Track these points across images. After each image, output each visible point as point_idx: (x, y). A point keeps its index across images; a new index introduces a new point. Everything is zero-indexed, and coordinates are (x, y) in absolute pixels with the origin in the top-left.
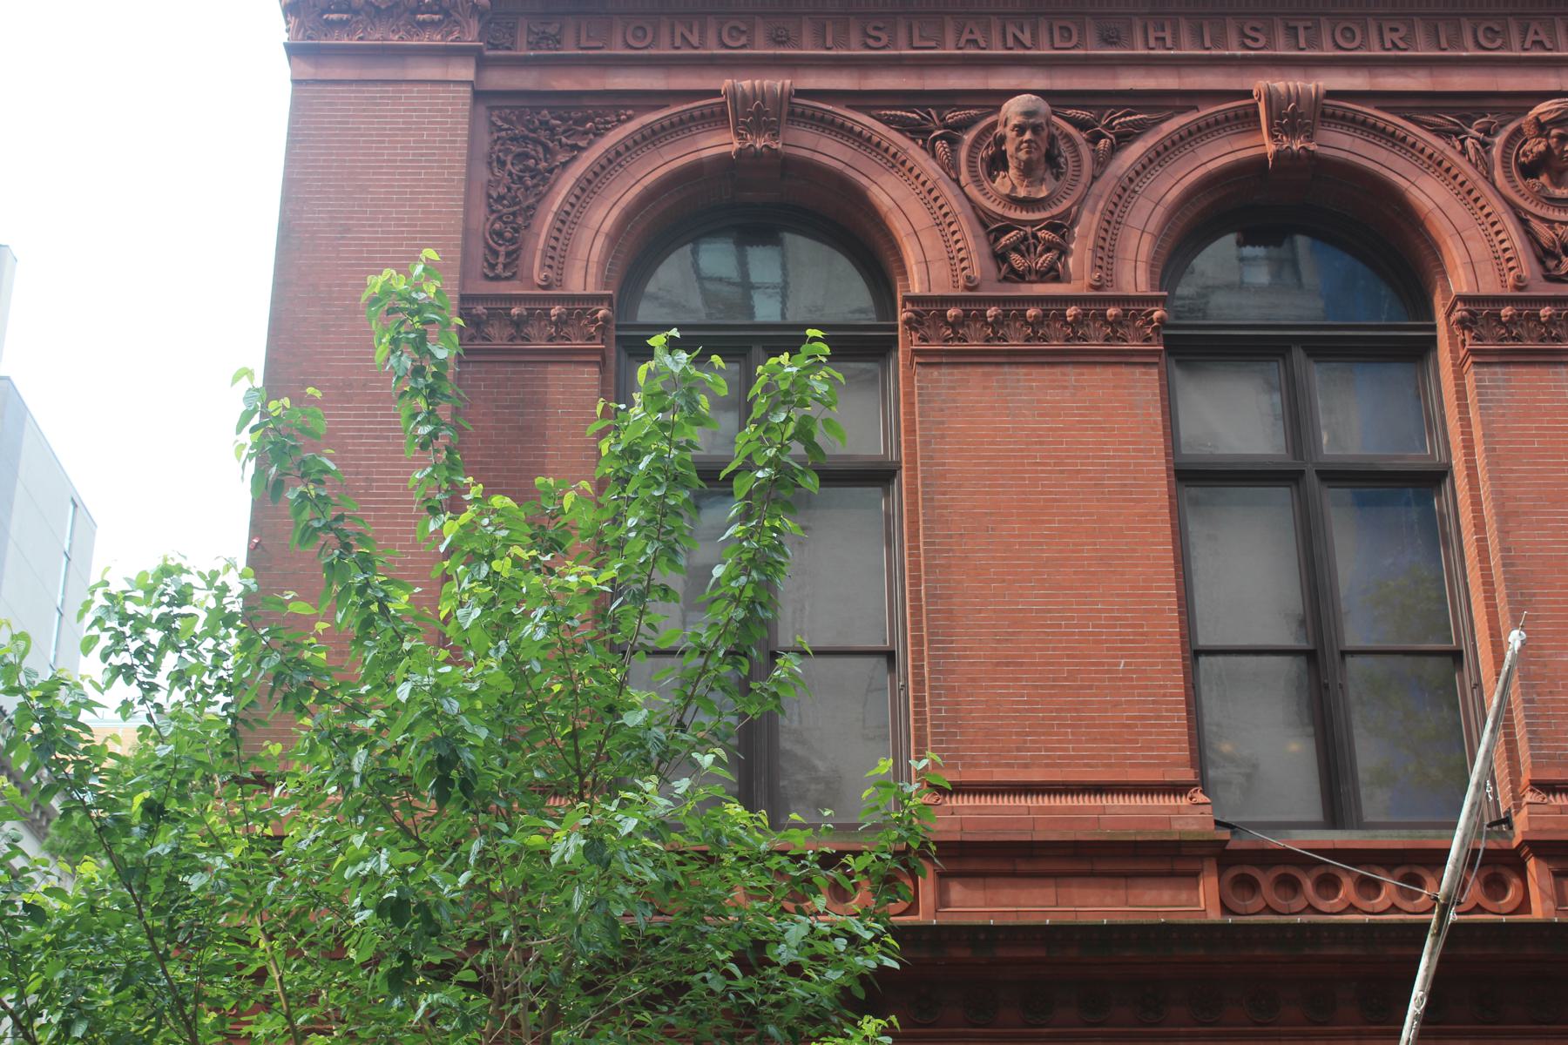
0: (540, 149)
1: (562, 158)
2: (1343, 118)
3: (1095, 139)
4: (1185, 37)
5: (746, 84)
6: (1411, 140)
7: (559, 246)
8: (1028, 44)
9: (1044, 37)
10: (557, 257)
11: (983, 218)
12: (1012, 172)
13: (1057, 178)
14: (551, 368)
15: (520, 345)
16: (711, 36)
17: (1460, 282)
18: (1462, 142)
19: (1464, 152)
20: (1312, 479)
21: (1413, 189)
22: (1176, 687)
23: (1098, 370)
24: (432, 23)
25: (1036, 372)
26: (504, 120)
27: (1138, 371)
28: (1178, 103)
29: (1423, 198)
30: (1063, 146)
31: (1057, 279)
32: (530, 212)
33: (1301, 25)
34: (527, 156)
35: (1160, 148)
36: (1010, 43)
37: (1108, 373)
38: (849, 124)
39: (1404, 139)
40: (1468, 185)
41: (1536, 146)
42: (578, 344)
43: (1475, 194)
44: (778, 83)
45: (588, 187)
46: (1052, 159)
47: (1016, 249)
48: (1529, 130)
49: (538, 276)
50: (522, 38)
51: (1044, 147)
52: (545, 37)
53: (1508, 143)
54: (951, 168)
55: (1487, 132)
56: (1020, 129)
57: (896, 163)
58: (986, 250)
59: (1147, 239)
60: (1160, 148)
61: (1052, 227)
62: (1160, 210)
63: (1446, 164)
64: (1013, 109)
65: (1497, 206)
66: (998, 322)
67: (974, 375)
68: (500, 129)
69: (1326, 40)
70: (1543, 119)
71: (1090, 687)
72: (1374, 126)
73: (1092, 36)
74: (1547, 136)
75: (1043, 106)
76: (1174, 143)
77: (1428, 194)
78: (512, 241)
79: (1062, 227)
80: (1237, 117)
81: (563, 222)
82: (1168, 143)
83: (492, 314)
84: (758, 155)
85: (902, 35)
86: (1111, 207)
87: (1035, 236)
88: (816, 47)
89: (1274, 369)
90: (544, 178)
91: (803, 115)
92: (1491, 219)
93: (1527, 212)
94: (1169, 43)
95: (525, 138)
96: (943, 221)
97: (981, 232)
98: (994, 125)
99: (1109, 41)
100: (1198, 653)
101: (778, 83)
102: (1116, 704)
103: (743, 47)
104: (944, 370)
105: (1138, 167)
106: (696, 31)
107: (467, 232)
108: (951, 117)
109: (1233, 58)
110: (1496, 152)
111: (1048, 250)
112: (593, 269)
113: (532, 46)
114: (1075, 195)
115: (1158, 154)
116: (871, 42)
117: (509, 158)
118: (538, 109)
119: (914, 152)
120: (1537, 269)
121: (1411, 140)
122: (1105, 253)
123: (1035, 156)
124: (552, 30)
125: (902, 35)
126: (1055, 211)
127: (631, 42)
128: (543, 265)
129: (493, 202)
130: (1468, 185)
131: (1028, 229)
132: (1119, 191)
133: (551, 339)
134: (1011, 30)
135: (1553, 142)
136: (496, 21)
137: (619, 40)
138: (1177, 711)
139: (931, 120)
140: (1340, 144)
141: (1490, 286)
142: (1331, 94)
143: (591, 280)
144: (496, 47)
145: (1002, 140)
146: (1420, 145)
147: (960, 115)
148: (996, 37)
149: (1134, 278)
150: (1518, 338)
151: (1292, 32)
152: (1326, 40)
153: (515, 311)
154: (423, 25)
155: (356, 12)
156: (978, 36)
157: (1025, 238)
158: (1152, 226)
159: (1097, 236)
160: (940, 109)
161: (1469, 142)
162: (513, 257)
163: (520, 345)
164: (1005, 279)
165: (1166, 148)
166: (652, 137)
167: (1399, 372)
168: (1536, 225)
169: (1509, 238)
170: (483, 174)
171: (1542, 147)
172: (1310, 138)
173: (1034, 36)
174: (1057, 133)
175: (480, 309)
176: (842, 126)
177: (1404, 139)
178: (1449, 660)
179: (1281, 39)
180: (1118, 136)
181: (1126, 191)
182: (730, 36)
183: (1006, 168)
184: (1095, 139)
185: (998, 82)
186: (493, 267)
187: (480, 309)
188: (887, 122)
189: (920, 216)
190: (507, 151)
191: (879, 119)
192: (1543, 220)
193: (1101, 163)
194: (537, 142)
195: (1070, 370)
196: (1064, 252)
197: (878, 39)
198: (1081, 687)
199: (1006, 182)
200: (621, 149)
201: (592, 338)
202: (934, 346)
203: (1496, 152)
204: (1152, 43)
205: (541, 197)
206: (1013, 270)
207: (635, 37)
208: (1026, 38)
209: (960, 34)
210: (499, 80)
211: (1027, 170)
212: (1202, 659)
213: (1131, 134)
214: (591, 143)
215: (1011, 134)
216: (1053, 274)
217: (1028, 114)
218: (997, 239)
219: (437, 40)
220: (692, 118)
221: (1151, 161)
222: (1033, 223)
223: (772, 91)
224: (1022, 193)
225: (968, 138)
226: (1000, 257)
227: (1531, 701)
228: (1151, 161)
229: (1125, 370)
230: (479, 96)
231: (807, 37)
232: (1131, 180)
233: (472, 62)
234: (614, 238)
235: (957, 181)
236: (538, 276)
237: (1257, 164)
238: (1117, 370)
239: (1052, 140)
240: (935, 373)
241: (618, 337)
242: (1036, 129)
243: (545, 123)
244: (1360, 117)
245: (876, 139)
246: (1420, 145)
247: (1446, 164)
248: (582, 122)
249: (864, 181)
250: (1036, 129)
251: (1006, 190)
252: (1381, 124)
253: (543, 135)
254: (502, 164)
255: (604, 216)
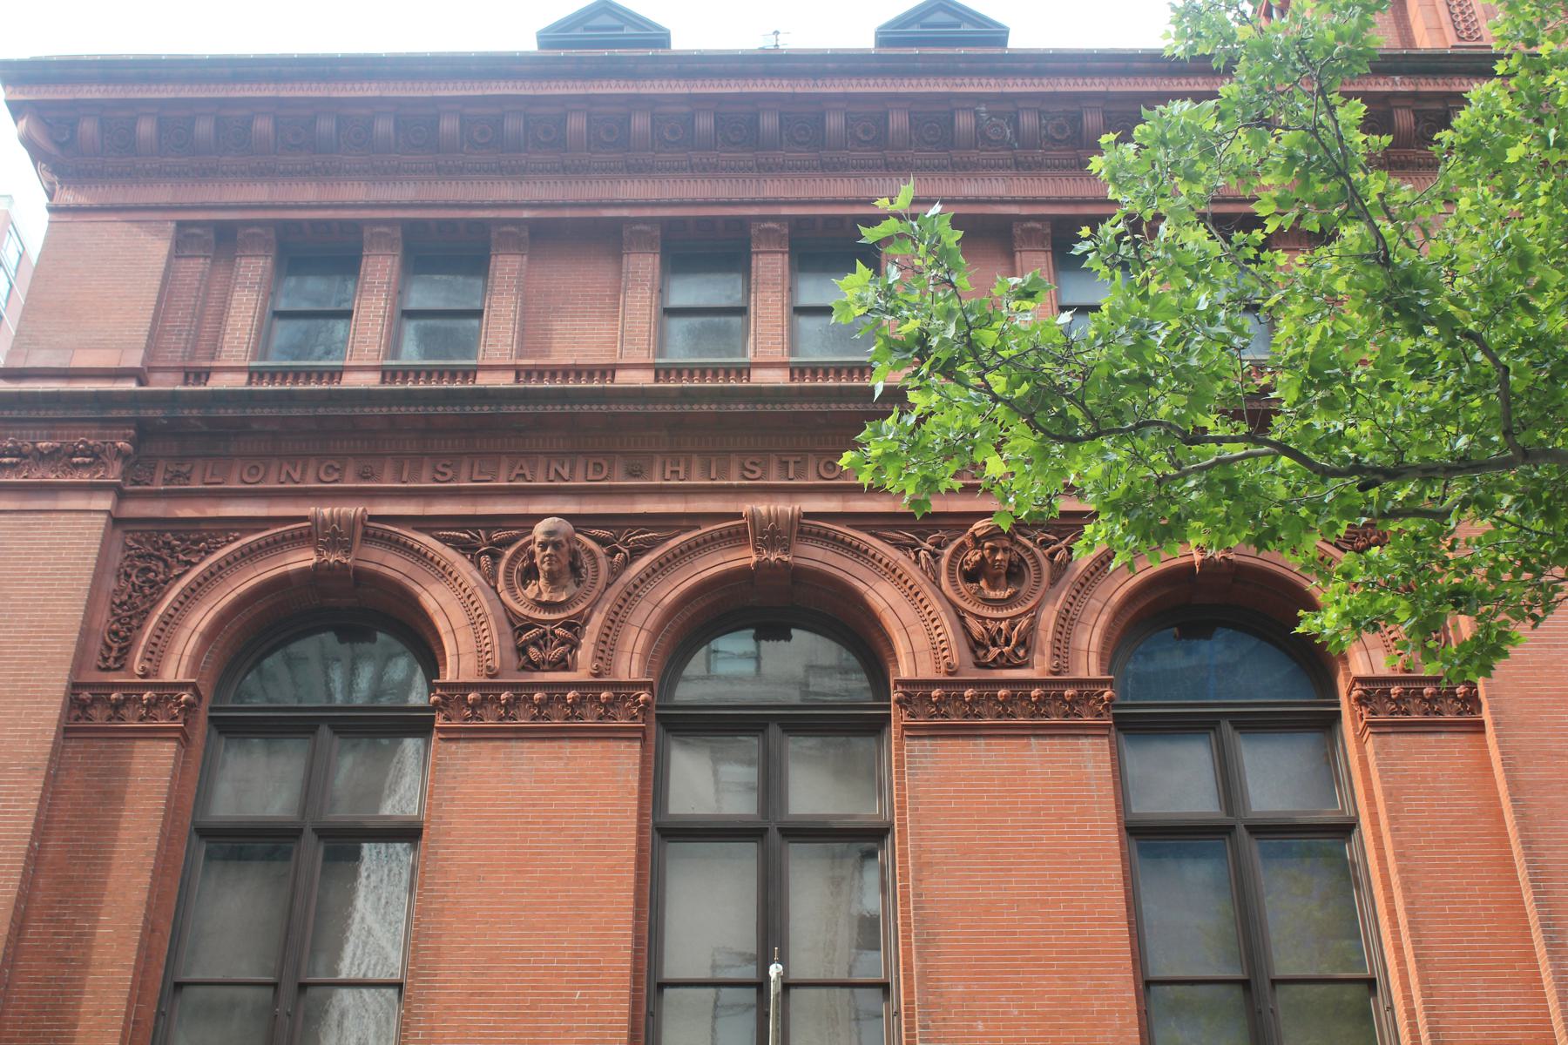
0: (161, 565)
1: (176, 572)
2: (389, 539)
3: (612, 553)
4: (696, 470)
5: (326, 511)
6: (871, 552)
7: (160, 642)
8: (566, 476)
9: (580, 471)
10: (156, 654)
11: (511, 617)
12: (542, 581)
13: (578, 585)
14: (138, 743)
15: (82, 723)
16: (311, 473)
17: (905, 670)
18: (917, 553)
19: (917, 561)
20: (774, 836)
21: (871, 592)
22: (622, 1014)
23: (590, 743)
24: (84, 464)
25: (538, 745)
26: (137, 541)
27: (623, 744)
28: (684, 523)
29: (879, 600)
30: (585, 559)
31: (566, 668)
32: (146, 614)
33: (791, 460)
34: (149, 570)
35: (663, 561)
36: (668, 475)
37: (595, 748)
38: (410, 542)
39: (866, 551)
40: (915, 589)
41: (974, 556)
42: (163, 723)
43: (920, 596)
44: (352, 510)
45: (191, 596)
46: (575, 569)
47: (535, 644)
48: (970, 544)
49: (137, 668)
50: (159, 475)
51: (565, 560)
52: (178, 475)
53: (955, 554)
54: (491, 577)
55: (938, 545)
56: (544, 546)
57: (444, 573)
58: (509, 643)
59: (644, 634)
60: (663, 561)
61: (568, 625)
62: (658, 610)
63: (899, 572)
64: (540, 529)
65: (937, 606)
66: (509, 705)
67: (485, 748)
68: (131, 548)
69: (811, 472)
70: (978, 534)
71: (548, 1015)
72: (842, 541)
73: (619, 470)
74: (982, 548)
75: (567, 526)
76: (675, 556)
77: (882, 596)
78: (125, 639)
79: (575, 626)
80: (730, 534)
81: (166, 623)
82: (670, 556)
83: (96, 699)
84: (331, 568)
85: (465, 470)
86: (616, 609)
87: (552, 632)
88: (702, 478)
89: (752, 743)
90: (158, 588)
91: (374, 535)
92: (933, 616)
93: (964, 611)
94: (682, 476)
95: (150, 556)
96: (475, 622)
97: (509, 630)
98: (529, 543)
99: (633, 474)
100: (662, 986)
101: (352, 510)
102: (568, 1030)
103: (335, 481)
104: (462, 744)
105: (643, 576)
106: (567, 469)
107: (86, 632)
108: (496, 536)
109: (197, 491)
110: (944, 562)
111: (562, 644)
112: (185, 662)
113: (166, 482)
114: (590, 599)
115: (661, 565)
116: (747, 474)
117: (134, 572)
118: (162, 533)
119: (461, 565)
120: (969, 658)
121: (871, 552)
122: (607, 647)
123: (555, 567)
124: (184, 469)
125: (465, 470)
126: (572, 612)
127: (246, 477)
128: (143, 659)
129: (116, 606)
130: (915, 589)
131: (548, 628)
132: (624, 595)
133: (141, 719)
134: (555, 465)
135: (986, 553)
136: (136, 463)
137: (236, 476)
138: (619, 1035)
139: (481, 540)
140: (815, 556)
141: (927, 672)
142: (808, 515)
143: (182, 670)
144: (137, 483)
145: (532, 555)
146: (879, 556)
147: (504, 534)
148: (540, 472)
149: (629, 666)
150: (946, 715)
151: (784, 465)
152: (811, 472)
153: (537, 696)
154: (77, 466)
155: (20, 455)
156: (526, 472)
157: (545, 634)
158: (648, 626)
159: (601, 633)
160: (488, 530)
161: (922, 554)
162: (125, 651)
163: (82, 723)
164: (524, 668)
165: (668, 561)
166: (250, 555)
167: (861, 744)
168: (970, 621)
169: (945, 632)
170: (111, 583)
171: (977, 557)
172: (786, 551)
173: (572, 470)
174: (578, 547)
175: (86, 694)
176: (405, 544)
177: (866, 551)
178: (878, 992)
179: (774, 469)
180: (631, 551)
181: (630, 597)
182: (327, 473)
183: (538, 578)
184: (612, 553)
185: (535, 509)
186: (106, 659)
187: (86, 694)
188: (444, 540)
189: (459, 616)
190: (133, 566)
191: (438, 538)
192: (978, 617)
193: (615, 573)
194: (160, 558)
195: (567, 744)
196: (575, 646)
197: (444, 474)
198: (541, 1015)
199: (539, 588)
200: (223, 564)
201: (174, 718)
202: (455, 724)
203: (944, 562)
204: (668, 475)
205: (155, 603)
206: (531, 662)
207: (250, 475)
208: (565, 472)
209: (512, 468)
210: (134, 509)
211: (553, 579)
212: (668, 992)
213: (641, 549)
214: (202, 559)
215: (538, 550)
216: (562, 664)
217: (549, 533)
218: (520, 636)
219: (86, 478)
220: (284, 539)
221: (654, 571)
222: (552, 622)
223: (346, 516)
224: (545, 597)
225: (509, 553)
226: (521, 650)
227: (927, 1027)
228: (654, 571)
229: (612, 744)
230: (116, 521)
231: (388, 472)
232: (636, 587)
233: (112, 495)
234: (210, 636)
235: (495, 588)
236: (137, 668)
237: (742, 574)
238: (606, 743)
239: (574, 555)
240: (453, 746)
241: (211, 718)
242: (556, 545)
243: (167, 544)
244: (832, 534)
245: (430, 554)
246: (879, 556)
247: (899, 572)
248: (196, 542)
249: (417, 589)
250: (556, 545)
251: (532, 596)
252: (848, 539)
253: (165, 552)
254: (128, 576)
255: (201, 618)
